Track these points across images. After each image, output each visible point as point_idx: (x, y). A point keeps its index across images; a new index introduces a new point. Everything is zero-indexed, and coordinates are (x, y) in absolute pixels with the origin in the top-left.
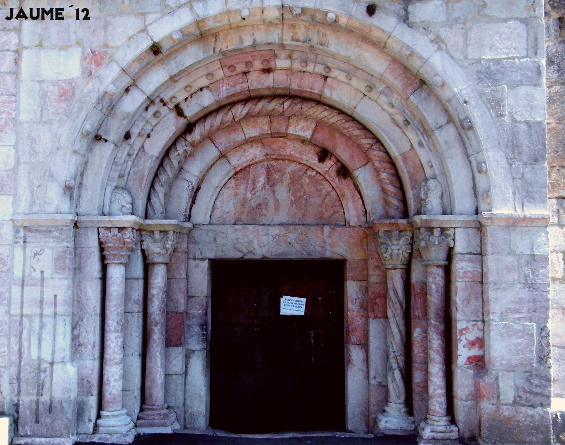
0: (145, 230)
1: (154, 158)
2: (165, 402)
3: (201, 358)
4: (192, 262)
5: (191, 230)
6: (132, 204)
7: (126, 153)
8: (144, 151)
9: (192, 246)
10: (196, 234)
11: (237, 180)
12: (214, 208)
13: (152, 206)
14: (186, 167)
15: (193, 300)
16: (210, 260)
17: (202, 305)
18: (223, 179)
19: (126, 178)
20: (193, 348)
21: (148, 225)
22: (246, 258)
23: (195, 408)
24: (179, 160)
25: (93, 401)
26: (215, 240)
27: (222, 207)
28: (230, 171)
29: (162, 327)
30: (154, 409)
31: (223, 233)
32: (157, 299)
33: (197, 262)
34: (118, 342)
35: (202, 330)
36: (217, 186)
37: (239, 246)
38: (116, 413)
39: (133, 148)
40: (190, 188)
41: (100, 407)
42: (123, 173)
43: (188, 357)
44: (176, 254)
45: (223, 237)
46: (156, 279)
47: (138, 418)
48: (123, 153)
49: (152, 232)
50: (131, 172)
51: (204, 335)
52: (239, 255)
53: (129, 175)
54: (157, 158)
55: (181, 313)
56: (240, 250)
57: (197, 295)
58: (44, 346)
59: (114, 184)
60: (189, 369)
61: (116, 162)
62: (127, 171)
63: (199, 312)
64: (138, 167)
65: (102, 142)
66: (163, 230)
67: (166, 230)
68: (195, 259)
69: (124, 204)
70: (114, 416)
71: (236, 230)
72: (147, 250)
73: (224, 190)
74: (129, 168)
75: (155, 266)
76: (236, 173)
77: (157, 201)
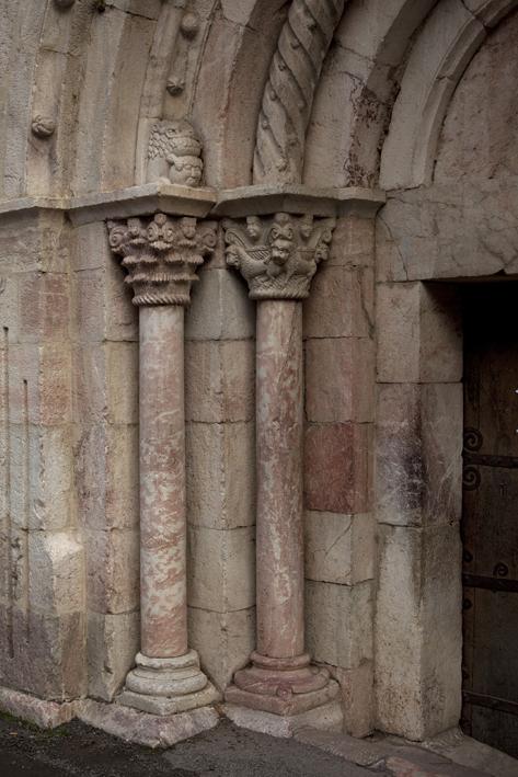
0: (228, 217)
1: (242, 30)
2: (306, 649)
3: (407, 547)
4: (385, 294)
5: (373, 211)
6: (201, 156)
7: (172, 30)
8: (223, 18)
9: (382, 250)
10: (392, 214)
11: (496, 51)
12: (440, 138)
13: (258, 153)
14: (348, 40)
15: (388, 392)
16: (425, 282)
17: (410, 407)
18: (450, 57)
19: (189, 92)
20: (390, 520)
21: (227, 204)
22: (509, 271)
23: (397, 679)
24: (311, 22)
25: (117, 626)
26: (436, 231)
27: (459, 134)
28: (469, 27)
29: (282, 462)
30: (265, 667)
31: (454, 206)
32: (268, 391)
33: (397, 290)
34: (160, 493)
35: (411, 473)
36: (440, 78)
37: (493, 240)
38: (175, 662)
39: (196, 14)
40: (358, 93)
41: (138, 643)
42: (174, 81)
43: (379, 542)
44: (330, 273)
45: (454, 219)
46: (266, 340)
47: (233, 682)
48: (164, 32)
49: (242, 221)
50: (201, 76)
51: (413, 487)
52: (490, 266)
53: (196, 82)
54: (251, 29)
55: (347, 427)
56: (497, 250)
57: (397, 379)
58: (14, 493)
59: (155, 111)
60: (383, 572)
61: (153, 57)
62: (190, 76)
63: (403, 424)
64: (211, 61)
65: (109, 15)
66: (261, 212)
67: (269, 212)
68: (391, 283)
69: (173, 157)
70: (156, 670)
71: (485, 195)
72: (240, 267)
73: (465, 87)
74: (193, 68)
75: (263, 305)
76: (491, 31)
77: (269, 141)
